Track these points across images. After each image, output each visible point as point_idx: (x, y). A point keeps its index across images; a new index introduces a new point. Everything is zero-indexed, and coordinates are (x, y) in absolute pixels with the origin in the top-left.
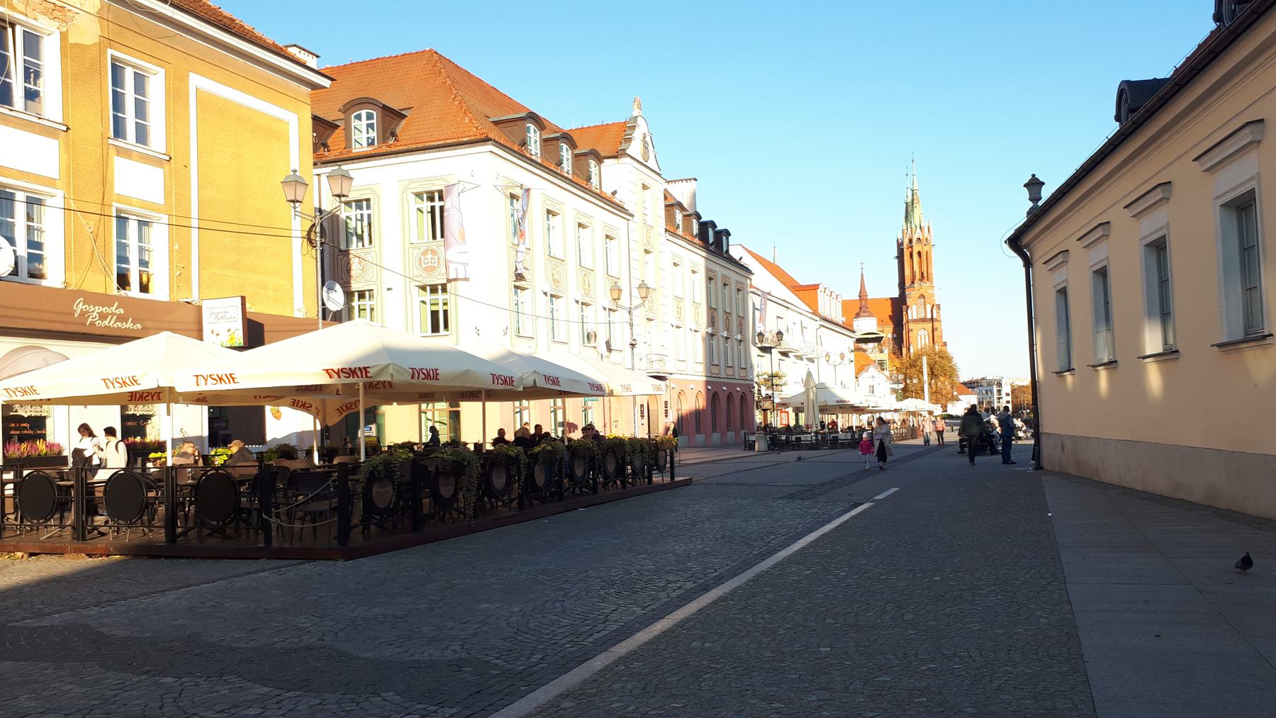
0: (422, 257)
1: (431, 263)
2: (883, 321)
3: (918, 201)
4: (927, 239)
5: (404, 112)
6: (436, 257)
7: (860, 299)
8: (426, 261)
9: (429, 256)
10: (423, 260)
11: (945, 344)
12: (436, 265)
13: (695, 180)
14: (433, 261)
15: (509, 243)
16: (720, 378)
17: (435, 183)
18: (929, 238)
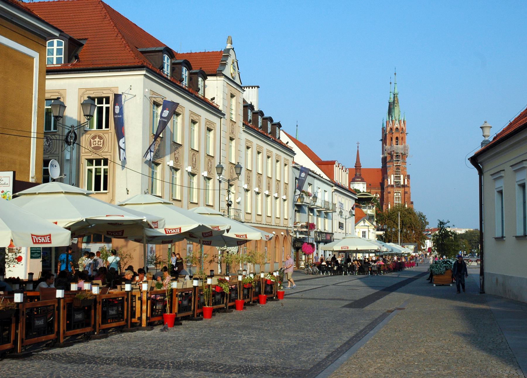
0: (92, 140)
1: (98, 144)
2: (370, 185)
3: (398, 102)
4: (402, 129)
5: (81, 42)
6: (102, 141)
7: (356, 169)
8: (94, 143)
9: (97, 139)
10: (92, 142)
11: (412, 203)
12: (101, 146)
13: (258, 87)
14: (99, 143)
15: (172, 141)
16: (271, 225)
17: (104, 92)
18: (404, 128)
